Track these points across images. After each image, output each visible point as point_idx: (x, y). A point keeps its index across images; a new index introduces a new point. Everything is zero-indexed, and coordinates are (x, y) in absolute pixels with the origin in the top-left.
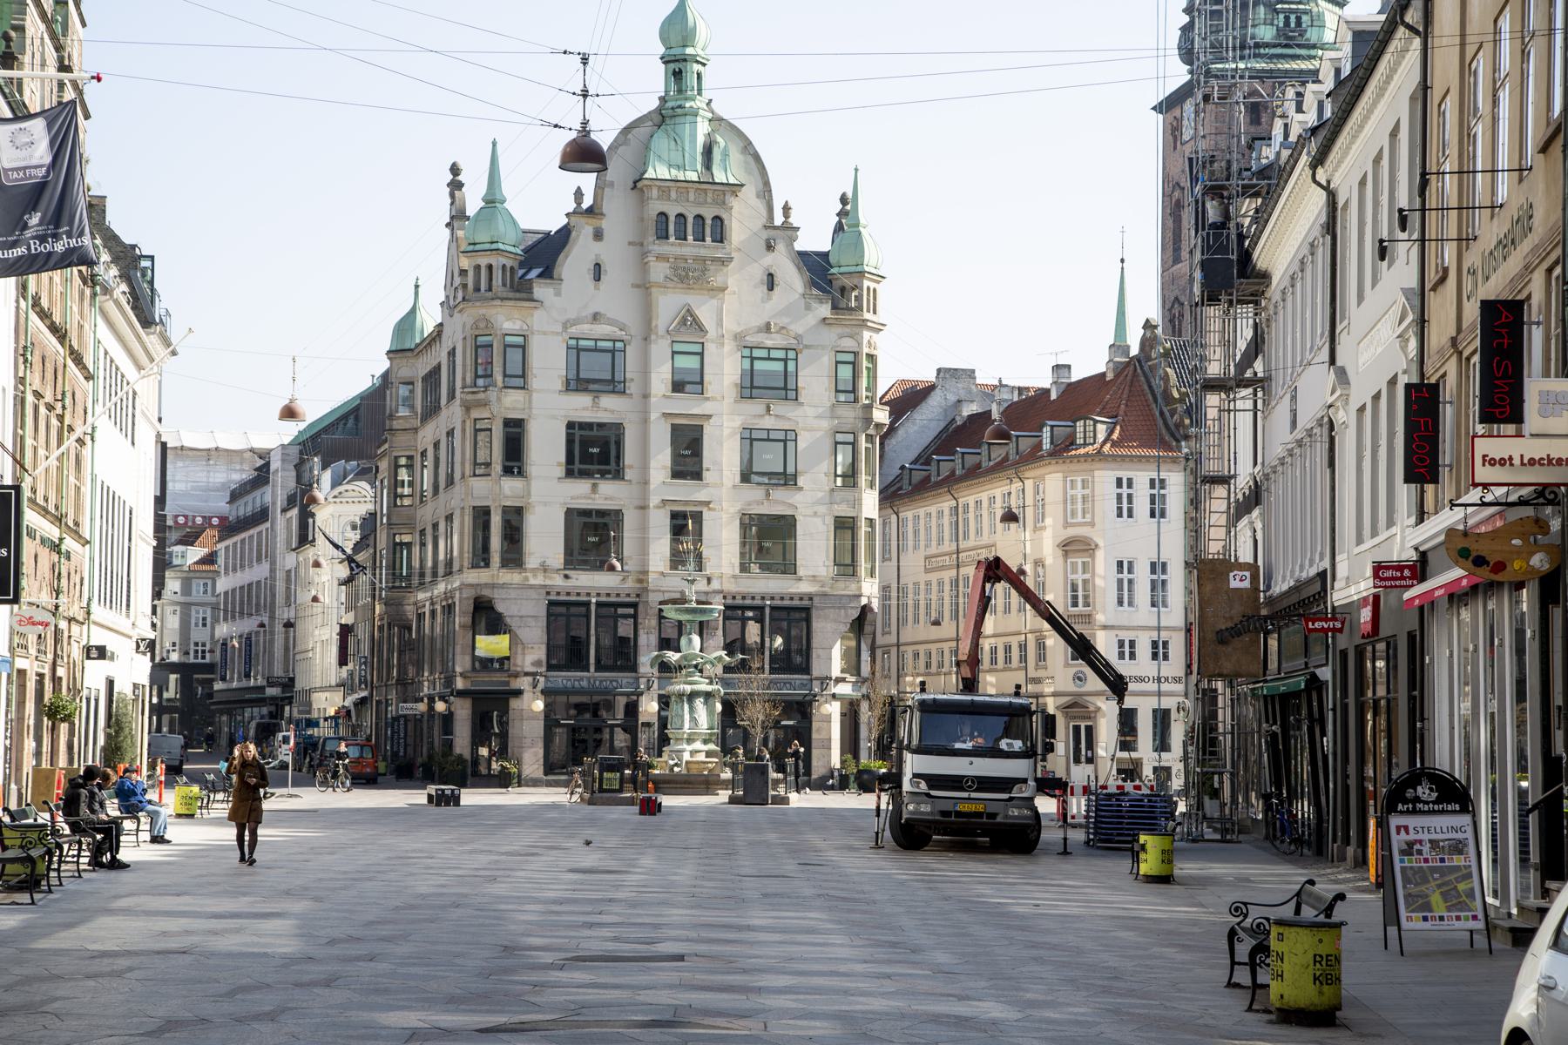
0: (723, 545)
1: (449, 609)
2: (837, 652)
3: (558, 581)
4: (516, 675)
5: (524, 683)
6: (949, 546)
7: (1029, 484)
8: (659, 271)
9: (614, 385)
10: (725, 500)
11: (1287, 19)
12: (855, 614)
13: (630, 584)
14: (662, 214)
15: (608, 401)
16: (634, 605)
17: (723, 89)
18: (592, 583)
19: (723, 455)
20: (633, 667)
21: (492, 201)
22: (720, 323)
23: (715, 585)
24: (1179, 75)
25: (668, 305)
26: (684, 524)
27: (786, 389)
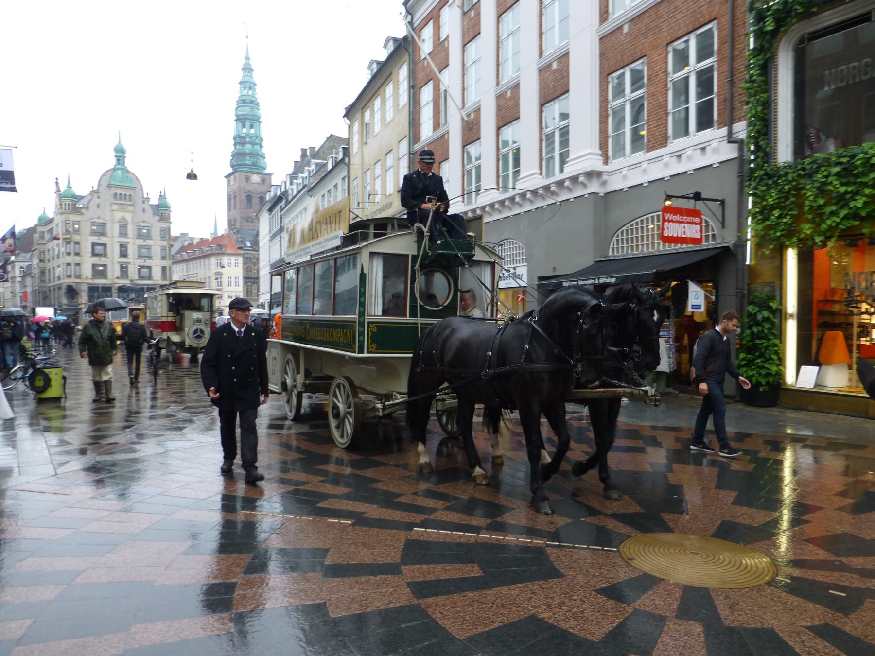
0: (133, 273)
1: (60, 288)
3: (91, 281)
5: (83, 306)
7: (206, 260)
9: (103, 234)
10: (133, 263)
14: (116, 194)
15: (102, 238)
17: (129, 164)
18: (100, 282)
19: (132, 250)
21: (69, 187)
24: (231, 170)
26: (124, 269)
27: (148, 236)
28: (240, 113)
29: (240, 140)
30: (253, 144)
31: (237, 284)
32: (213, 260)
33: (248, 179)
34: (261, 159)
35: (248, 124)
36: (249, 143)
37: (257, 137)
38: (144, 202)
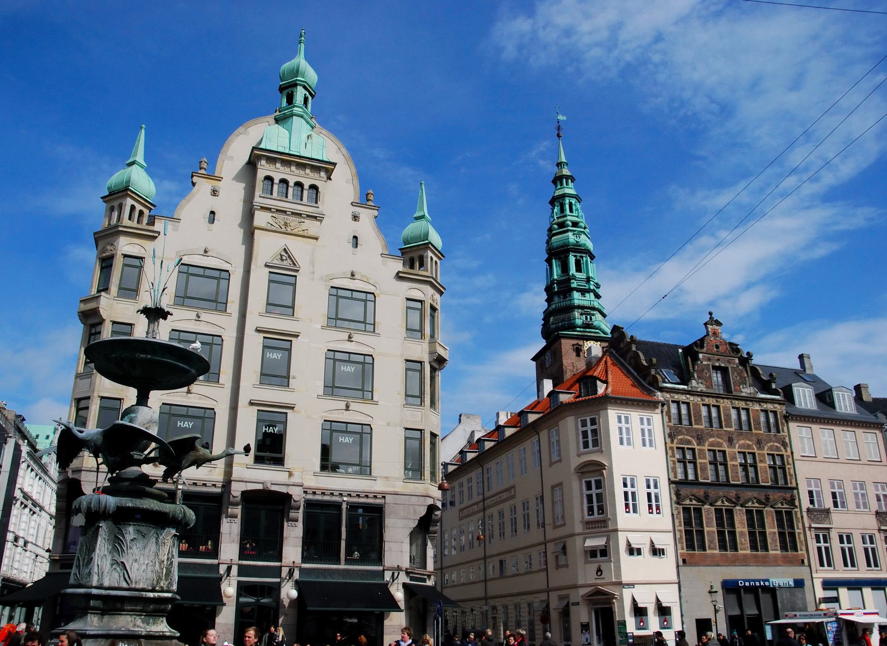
2: (406, 546)
6: (477, 498)
7: (544, 434)
8: (261, 219)
11: (586, 318)
12: (423, 511)
22: (312, 263)
23: (295, 479)
24: (543, 343)
25: (268, 246)
27: (368, 325)
28: (555, 245)
29: (559, 291)
30: (583, 292)
31: (654, 506)
32: (570, 426)
33: (578, 350)
34: (598, 316)
35: (572, 260)
36: (578, 290)
37: (588, 280)
38: (355, 218)
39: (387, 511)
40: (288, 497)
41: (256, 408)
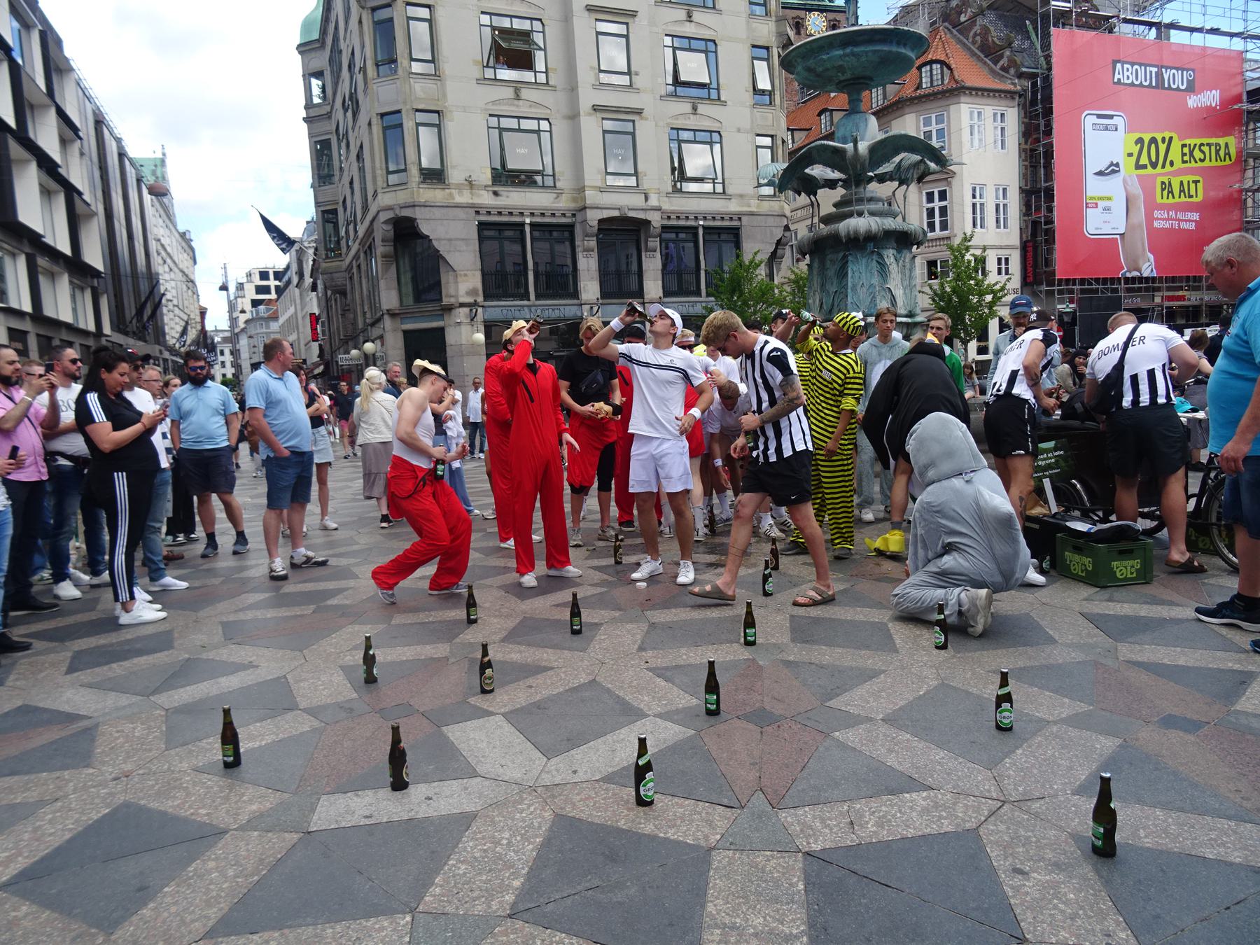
3: (486, 199)
4: (449, 309)
13: (565, 203)
16: (570, 228)
20: (575, 294)
23: (654, 201)
39: (744, 234)
40: (647, 223)
41: (600, 115)
